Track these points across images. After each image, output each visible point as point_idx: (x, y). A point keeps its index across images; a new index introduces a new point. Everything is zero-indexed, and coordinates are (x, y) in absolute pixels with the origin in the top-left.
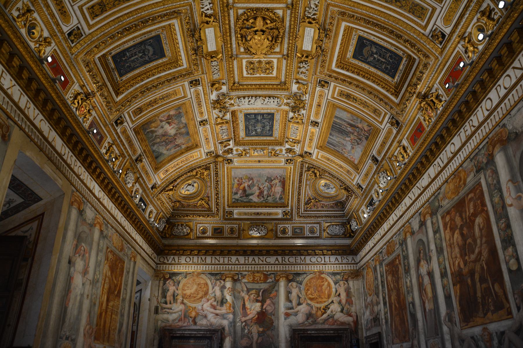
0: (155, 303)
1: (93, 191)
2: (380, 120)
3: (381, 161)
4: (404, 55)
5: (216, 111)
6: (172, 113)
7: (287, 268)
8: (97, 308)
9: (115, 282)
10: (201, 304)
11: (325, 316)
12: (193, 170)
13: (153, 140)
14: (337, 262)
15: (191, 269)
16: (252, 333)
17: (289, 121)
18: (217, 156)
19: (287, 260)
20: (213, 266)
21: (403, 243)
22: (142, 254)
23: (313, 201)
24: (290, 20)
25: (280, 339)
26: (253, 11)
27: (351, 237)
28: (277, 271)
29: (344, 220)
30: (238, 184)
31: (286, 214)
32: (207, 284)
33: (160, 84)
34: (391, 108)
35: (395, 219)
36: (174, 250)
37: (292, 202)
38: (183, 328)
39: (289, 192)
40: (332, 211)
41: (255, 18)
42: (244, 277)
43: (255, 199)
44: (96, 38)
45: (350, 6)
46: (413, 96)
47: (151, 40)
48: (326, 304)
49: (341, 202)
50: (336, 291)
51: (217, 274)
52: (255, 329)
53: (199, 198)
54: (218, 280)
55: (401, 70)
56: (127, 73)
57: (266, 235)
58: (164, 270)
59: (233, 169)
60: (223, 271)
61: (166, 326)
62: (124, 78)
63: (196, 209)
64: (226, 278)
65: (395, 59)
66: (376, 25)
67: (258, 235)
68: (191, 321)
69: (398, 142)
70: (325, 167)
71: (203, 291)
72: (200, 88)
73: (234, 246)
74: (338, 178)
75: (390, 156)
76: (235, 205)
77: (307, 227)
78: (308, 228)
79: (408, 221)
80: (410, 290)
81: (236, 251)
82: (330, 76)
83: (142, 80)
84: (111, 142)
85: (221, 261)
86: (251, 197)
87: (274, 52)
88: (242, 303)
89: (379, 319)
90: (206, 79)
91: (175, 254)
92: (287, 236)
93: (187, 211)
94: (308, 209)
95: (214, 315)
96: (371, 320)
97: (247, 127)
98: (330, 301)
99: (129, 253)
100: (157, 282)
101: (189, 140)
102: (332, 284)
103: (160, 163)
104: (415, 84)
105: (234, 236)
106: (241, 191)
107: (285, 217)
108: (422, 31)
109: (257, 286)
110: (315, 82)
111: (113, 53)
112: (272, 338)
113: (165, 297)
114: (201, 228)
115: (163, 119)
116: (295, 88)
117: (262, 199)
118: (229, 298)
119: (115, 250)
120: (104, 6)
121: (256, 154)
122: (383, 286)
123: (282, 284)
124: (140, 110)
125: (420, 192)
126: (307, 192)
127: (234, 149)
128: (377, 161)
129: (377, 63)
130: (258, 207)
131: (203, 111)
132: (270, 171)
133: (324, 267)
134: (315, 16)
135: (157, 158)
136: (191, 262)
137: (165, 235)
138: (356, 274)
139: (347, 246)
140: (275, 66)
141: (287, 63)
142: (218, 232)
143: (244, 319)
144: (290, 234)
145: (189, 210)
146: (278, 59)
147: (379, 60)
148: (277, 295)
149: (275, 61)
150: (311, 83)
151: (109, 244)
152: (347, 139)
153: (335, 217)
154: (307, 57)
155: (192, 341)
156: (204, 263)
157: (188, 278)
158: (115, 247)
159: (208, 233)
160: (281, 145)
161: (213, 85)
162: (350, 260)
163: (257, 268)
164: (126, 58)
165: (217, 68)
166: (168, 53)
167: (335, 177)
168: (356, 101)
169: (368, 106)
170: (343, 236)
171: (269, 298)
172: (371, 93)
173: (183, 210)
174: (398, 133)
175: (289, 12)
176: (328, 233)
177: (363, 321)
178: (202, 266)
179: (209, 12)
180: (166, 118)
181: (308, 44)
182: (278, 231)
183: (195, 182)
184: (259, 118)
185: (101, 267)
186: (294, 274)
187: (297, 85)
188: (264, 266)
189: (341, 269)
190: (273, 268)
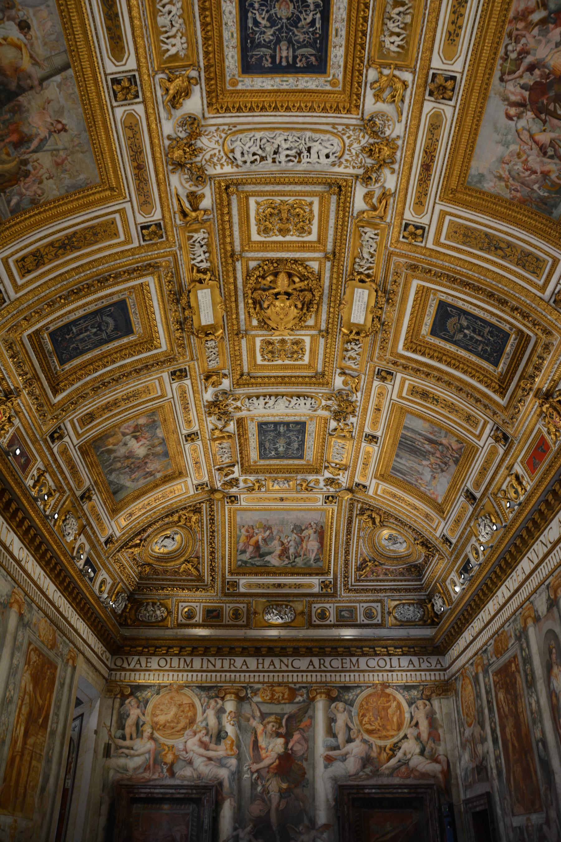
0: (105, 738)
1: (11, 549)
2: (477, 433)
3: (481, 499)
4: (511, 330)
5: (213, 419)
6: (142, 421)
7: (328, 677)
8: (6, 748)
9: (41, 702)
10: (183, 739)
11: (393, 761)
12: (173, 513)
13: (111, 465)
14: (411, 667)
15: (167, 679)
16: (268, 793)
17: (330, 435)
18: (213, 491)
19: (327, 664)
20: (204, 674)
21: (522, 635)
22: (86, 653)
23: (369, 564)
24: (331, 278)
25: (317, 803)
26: (272, 263)
27: (433, 624)
28: (311, 683)
29: (422, 595)
30: (247, 537)
31: (326, 586)
32: (193, 705)
33: (124, 375)
34: (495, 413)
35: (508, 594)
36: (140, 646)
37: (335, 565)
38: (151, 783)
39: (330, 550)
40: (401, 581)
41: (276, 275)
42: (255, 692)
43: (274, 560)
44: (25, 305)
45: (424, 255)
46: (528, 394)
47: (112, 309)
48: (395, 740)
49: (416, 566)
50: (412, 718)
51: (210, 688)
52: (274, 786)
53: (183, 559)
54: (212, 698)
55: (508, 354)
56: (72, 358)
57: (293, 621)
58: (122, 681)
59: (238, 512)
60: (221, 682)
61: (122, 780)
62: (67, 367)
63: (178, 577)
64: (226, 694)
65: (497, 336)
66: (467, 285)
67: (280, 621)
68: (165, 770)
69: (507, 468)
70: (388, 508)
71: (186, 717)
72: (188, 382)
73: (239, 640)
74: (410, 527)
75: (496, 491)
76: (241, 571)
77: (361, 608)
78: (362, 609)
79: (528, 599)
80: (538, 719)
81: (244, 648)
82: (395, 363)
83: (95, 370)
84: (43, 468)
85: (218, 667)
86: (268, 558)
87: (306, 327)
88: (253, 738)
89: (486, 768)
90: (197, 369)
91: (141, 654)
92: (328, 622)
93: (163, 580)
94: (362, 578)
95: (204, 759)
96: (473, 769)
97: (261, 445)
98: (401, 735)
99: (66, 651)
100: (110, 701)
101: (168, 464)
102: (405, 705)
103: (120, 501)
104: (530, 376)
105: (241, 623)
106: (251, 549)
107: (324, 591)
108: (539, 294)
109: (277, 709)
110: (372, 373)
111: (52, 328)
112: (303, 802)
113: (121, 726)
114: (186, 610)
115: (127, 431)
116: (338, 382)
117: (287, 561)
118: (230, 729)
119: (42, 646)
120: (42, 257)
121: (276, 487)
122: (491, 710)
123: (320, 704)
124: (91, 417)
125: (546, 550)
126: (360, 549)
127: (241, 479)
128: (474, 498)
129: (470, 343)
130: (280, 574)
131: (192, 418)
132: (300, 514)
133: (390, 677)
134: (370, 272)
135: (115, 493)
136: (167, 667)
137: (126, 620)
138: (445, 688)
139: (428, 639)
140: (308, 348)
141: (326, 344)
142: (213, 617)
143: (255, 767)
144: (332, 619)
145: (167, 580)
146: (312, 336)
147: (472, 338)
148: (312, 725)
150: (365, 374)
151: (32, 636)
152: (424, 463)
153: (406, 590)
154: (358, 333)
155: (166, 807)
156: (189, 668)
157: (161, 694)
158: (43, 642)
159: (197, 618)
160: (317, 473)
161: (207, 378)
162: (434, 664)
163: (278, 678)
165: (214, 351)
166: (137, 328)
167: (406, 525)
169: (457, 411)
170: (421, 623)
171: (298, 729)
172: (461, 389)
173: (156, 579)
174: (506, 454)
175: (328, 264)
176: (395, 618)
177: (458, 771)
178: (185, 674)
179: (204, 265)
180: (132, 429)
182: (313, 614)
183: (176, 533)
184: (282, 429)
185: (18, 676)
186: (341, 687)
187: (343, 378)
188: (290, 674)
189: (419, 679)
190: (304, 677)
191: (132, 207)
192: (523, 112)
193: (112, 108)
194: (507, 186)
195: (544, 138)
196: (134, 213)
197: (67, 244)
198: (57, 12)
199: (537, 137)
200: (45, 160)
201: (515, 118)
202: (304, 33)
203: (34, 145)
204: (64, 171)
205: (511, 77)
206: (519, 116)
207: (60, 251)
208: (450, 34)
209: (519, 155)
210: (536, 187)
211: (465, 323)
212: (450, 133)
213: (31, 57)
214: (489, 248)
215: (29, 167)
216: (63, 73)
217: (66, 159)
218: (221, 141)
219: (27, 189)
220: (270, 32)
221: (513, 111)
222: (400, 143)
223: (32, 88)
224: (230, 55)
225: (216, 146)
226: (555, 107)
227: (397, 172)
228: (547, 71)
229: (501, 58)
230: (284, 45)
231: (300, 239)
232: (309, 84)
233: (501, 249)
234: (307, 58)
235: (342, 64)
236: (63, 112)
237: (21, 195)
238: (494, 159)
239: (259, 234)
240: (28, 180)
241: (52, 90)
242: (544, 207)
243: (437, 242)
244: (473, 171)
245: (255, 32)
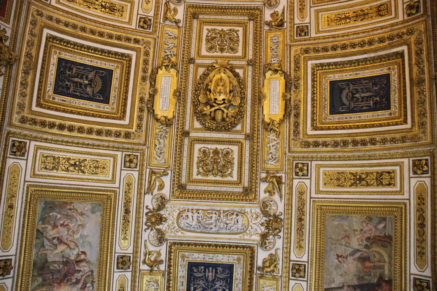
4: (54, 98)
26: (225, 129)
62: (385, 71)
65: (63, 87)
82: (137, 41)
120: (377, 179)
140: (204, 42)
147: (82, 78)
149: (204, 52)
161: (281, 25)
164: (375, 99)
168: (102, 5)
179: (272, 136)
181: (167, 81)
187: (177, 17)
191: (310, 193)
192: (77, 258)
193: (308, 262)
194: (77, 211)
195: (62, 248)
196: (310, 189)
197: (358, 180)
199: (65, 246)
200: (355, 243)
201: (80, 253)
203: (358, 255)
204: (346, 231)
205: (88, 274)
206: (78, 255)
207: (364, 176)
209: (74, 232)
210: (59, 216)
211: (89, 89)
212: (116, 237)
214: (80, 163)
215: (365, 243)
216: (329, 287)
217: (342, 238)
218: (250, 228)
219: (371, 230)
220: (217, 286)
221: (83, 257)
222: (145, 227)
223: (349, 286)
224: (239, 275)
225: (253, 225)
227: (145, 207)
230: (210, 279)
231: (206, 146)
232: (197, 256)
233: (72, 165)
234: (198, 271)
235: (179, 267)
236: (336, 266)
237: (376, 227)
238: (88, 225)
239: (232, 151)
240: (369, 235)
242: (50, 206)
243: (115, 157)
244: (99, 214)
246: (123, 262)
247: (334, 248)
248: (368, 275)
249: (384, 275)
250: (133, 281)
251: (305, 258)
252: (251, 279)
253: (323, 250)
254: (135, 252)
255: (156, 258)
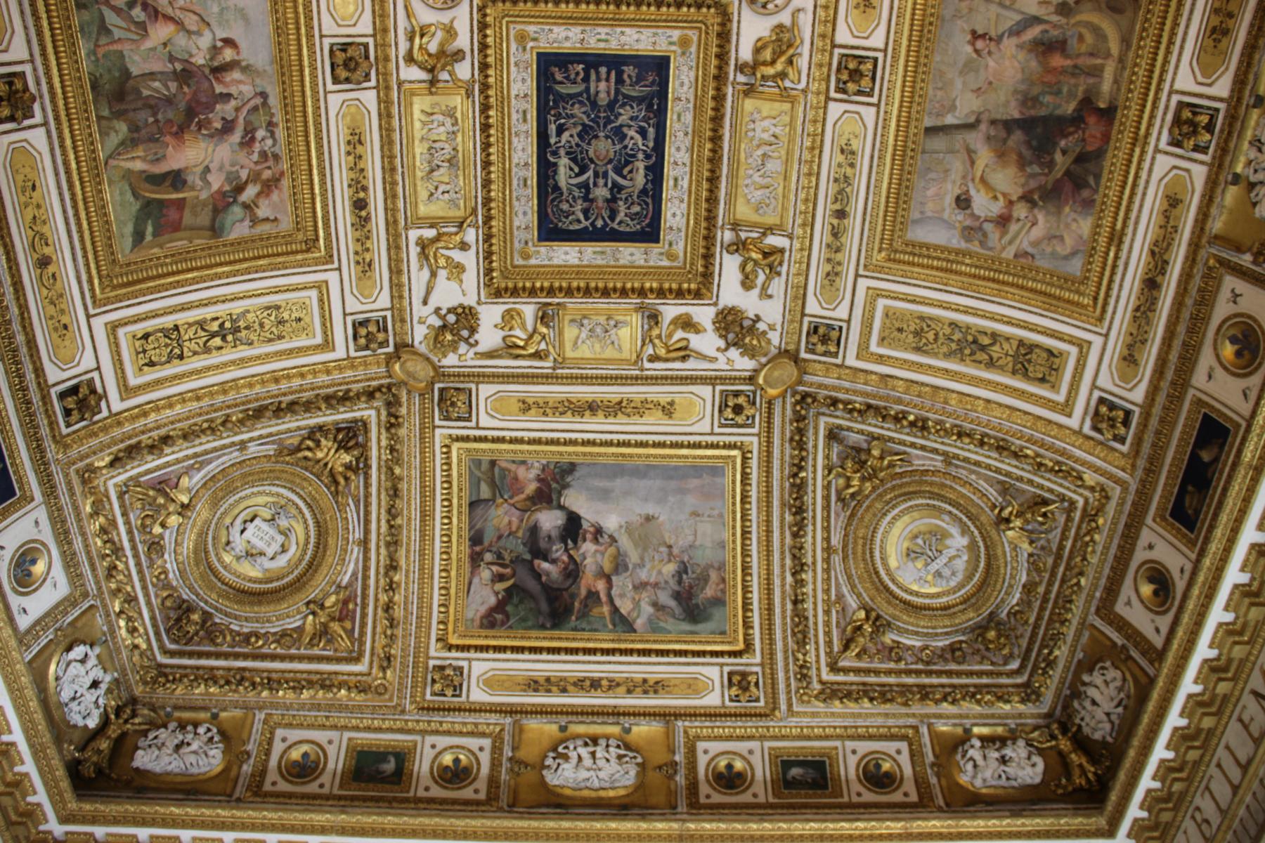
192: (212, 59)
193: (885, 51)
195: (161, 32)
198: (913, 203)
201: (219, 44)
202: (573, 116)
203: (1034, 32)
205: (252, 103)
208: (360, 142)
213: (973, 163)
216: (939, 123)
221: (228, 55)
223: (993, 122)
224: (685, 88)
226: (168, 88)
228: (204, 132)
229: (276, 125)
230: (603, 99)
232: (563, 35)
234: (567, 78)
235: (513, 69)
241: (966, 106)
245: (646, 119)
246: (349, 63)
247: (965, 11)
248: (1051, 93)
249: (1098, 93)
250: (385, 115)
251: (877, 40)
252: (719, 98)
253: (932, 15)
254: (381, 30)
255: (442, 45)
